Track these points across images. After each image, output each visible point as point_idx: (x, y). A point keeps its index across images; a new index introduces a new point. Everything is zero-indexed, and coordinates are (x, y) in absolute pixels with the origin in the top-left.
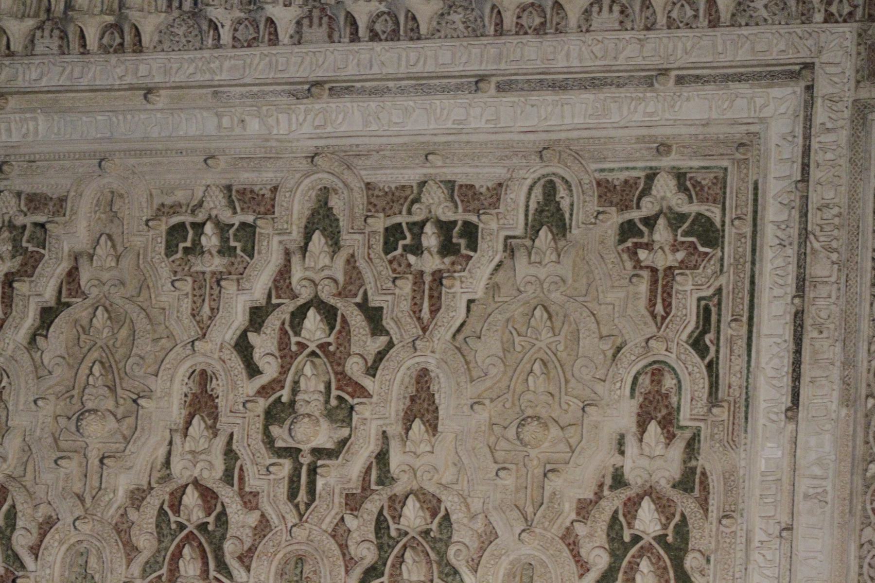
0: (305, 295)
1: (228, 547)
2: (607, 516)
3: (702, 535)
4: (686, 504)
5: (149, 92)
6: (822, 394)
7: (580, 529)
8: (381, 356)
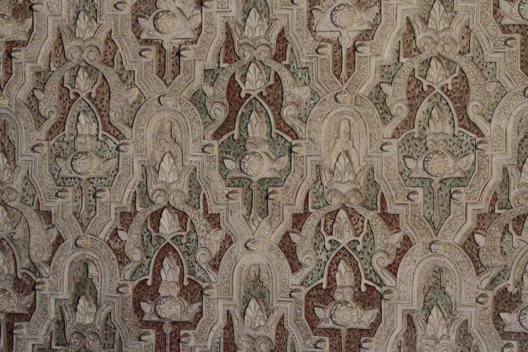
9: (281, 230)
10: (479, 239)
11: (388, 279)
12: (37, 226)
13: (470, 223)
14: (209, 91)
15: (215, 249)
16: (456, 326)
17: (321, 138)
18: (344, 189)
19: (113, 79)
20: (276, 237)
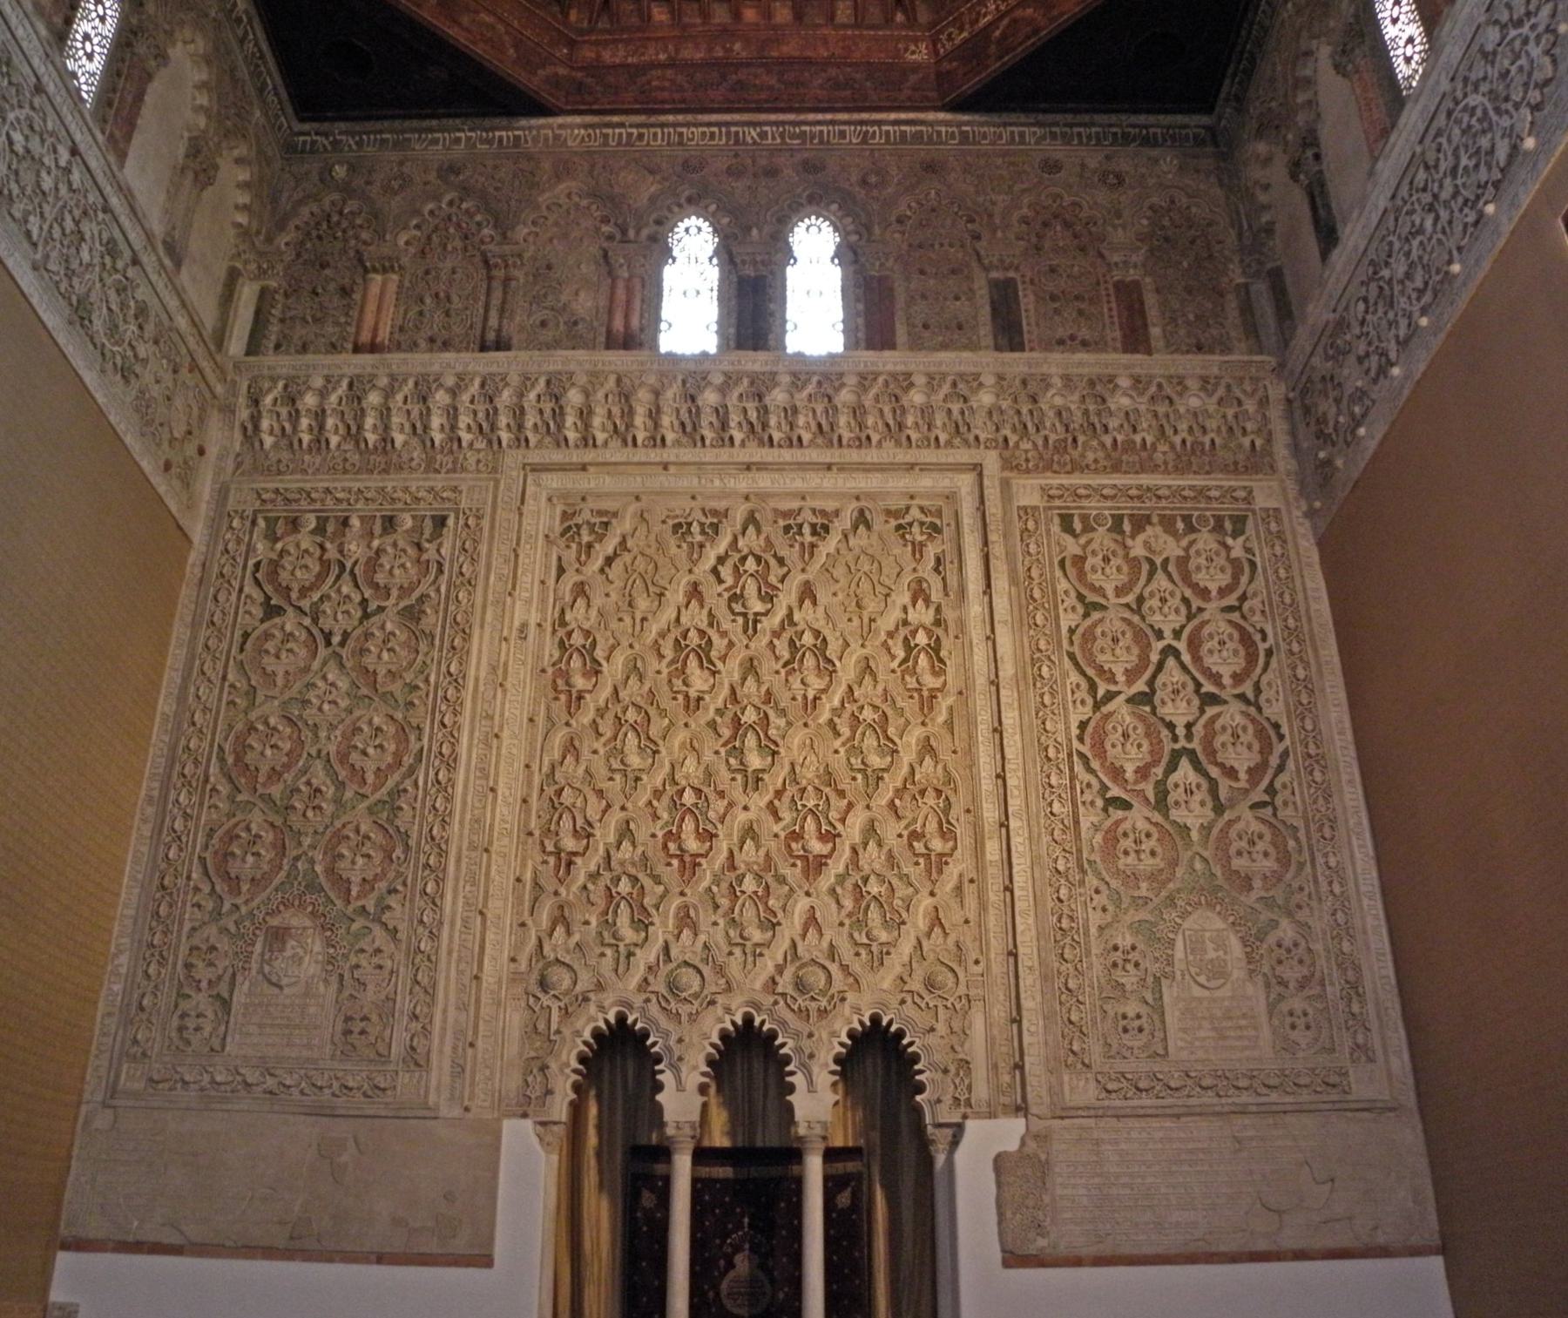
0: (746, 551)
1: (713, 654)
2: (901, 638)
3: (947, 644)
4: (940, 632)
5: (665, 468)
6: (1001, 582)
7: (890, 642)
8: (784, 577)
9: (767, 798)
10: (897, 802)
11: (839, 826)
12: (592, 798)
13: (891, 794)
14: (719, 720)
15: (722, 811)
16: (885, 849)
17: (795, 747)
18: (810, 776)
19: (652, 712)
20: (763, 803)
